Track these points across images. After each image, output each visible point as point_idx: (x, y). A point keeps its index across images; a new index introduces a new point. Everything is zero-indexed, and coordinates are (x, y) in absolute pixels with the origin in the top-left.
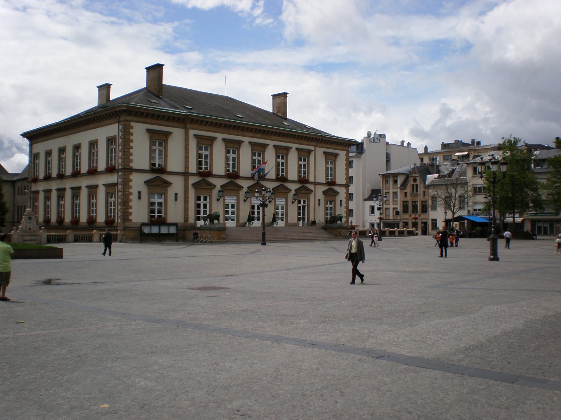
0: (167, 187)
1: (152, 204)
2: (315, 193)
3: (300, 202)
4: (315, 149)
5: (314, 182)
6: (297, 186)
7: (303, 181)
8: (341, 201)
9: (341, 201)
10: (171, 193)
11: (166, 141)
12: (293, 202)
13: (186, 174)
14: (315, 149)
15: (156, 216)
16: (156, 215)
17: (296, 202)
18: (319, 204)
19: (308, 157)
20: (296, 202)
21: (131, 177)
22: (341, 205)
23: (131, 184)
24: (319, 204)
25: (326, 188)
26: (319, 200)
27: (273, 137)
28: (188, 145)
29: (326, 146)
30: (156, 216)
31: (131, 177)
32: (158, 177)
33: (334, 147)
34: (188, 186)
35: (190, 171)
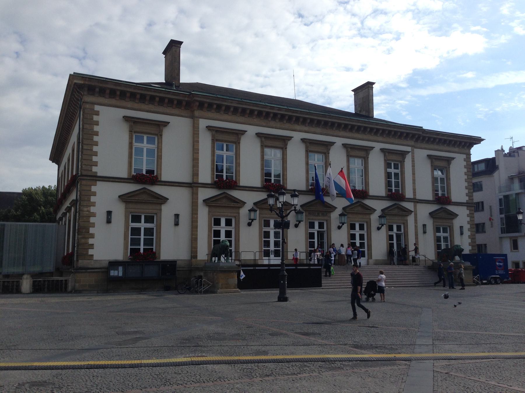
0: (161, 204)
1: (136, 231)
2: (416, 215)
3: (391, 228)
4: (413, 150)
5: (414, 199)
6: (386, 204)
7: (395, 196)
8: (461, 227)
9: (461, 227)
10: (167, 213)
11: (160, 135)
12: (379, 229)
13: (193, 186)
14: (413, 150)
15: (142, 251)
16: (142, 247)
17: (384, 228)
18: (425, 232)
19: (402, 162)
20: (384, 228)
21: (93, 189)
22: (462, 234)
23: (93, 199)
24: (425, 232)
25: (434, 207)
26: (424, 226)
27: (342, 133)
28: (198, 142)
29: (432, 146)
30: (142, 251)
31: (93, 189)
32: (395, 204)
33: (446, 148)
34: (197, 202)
35: (200, 181)
